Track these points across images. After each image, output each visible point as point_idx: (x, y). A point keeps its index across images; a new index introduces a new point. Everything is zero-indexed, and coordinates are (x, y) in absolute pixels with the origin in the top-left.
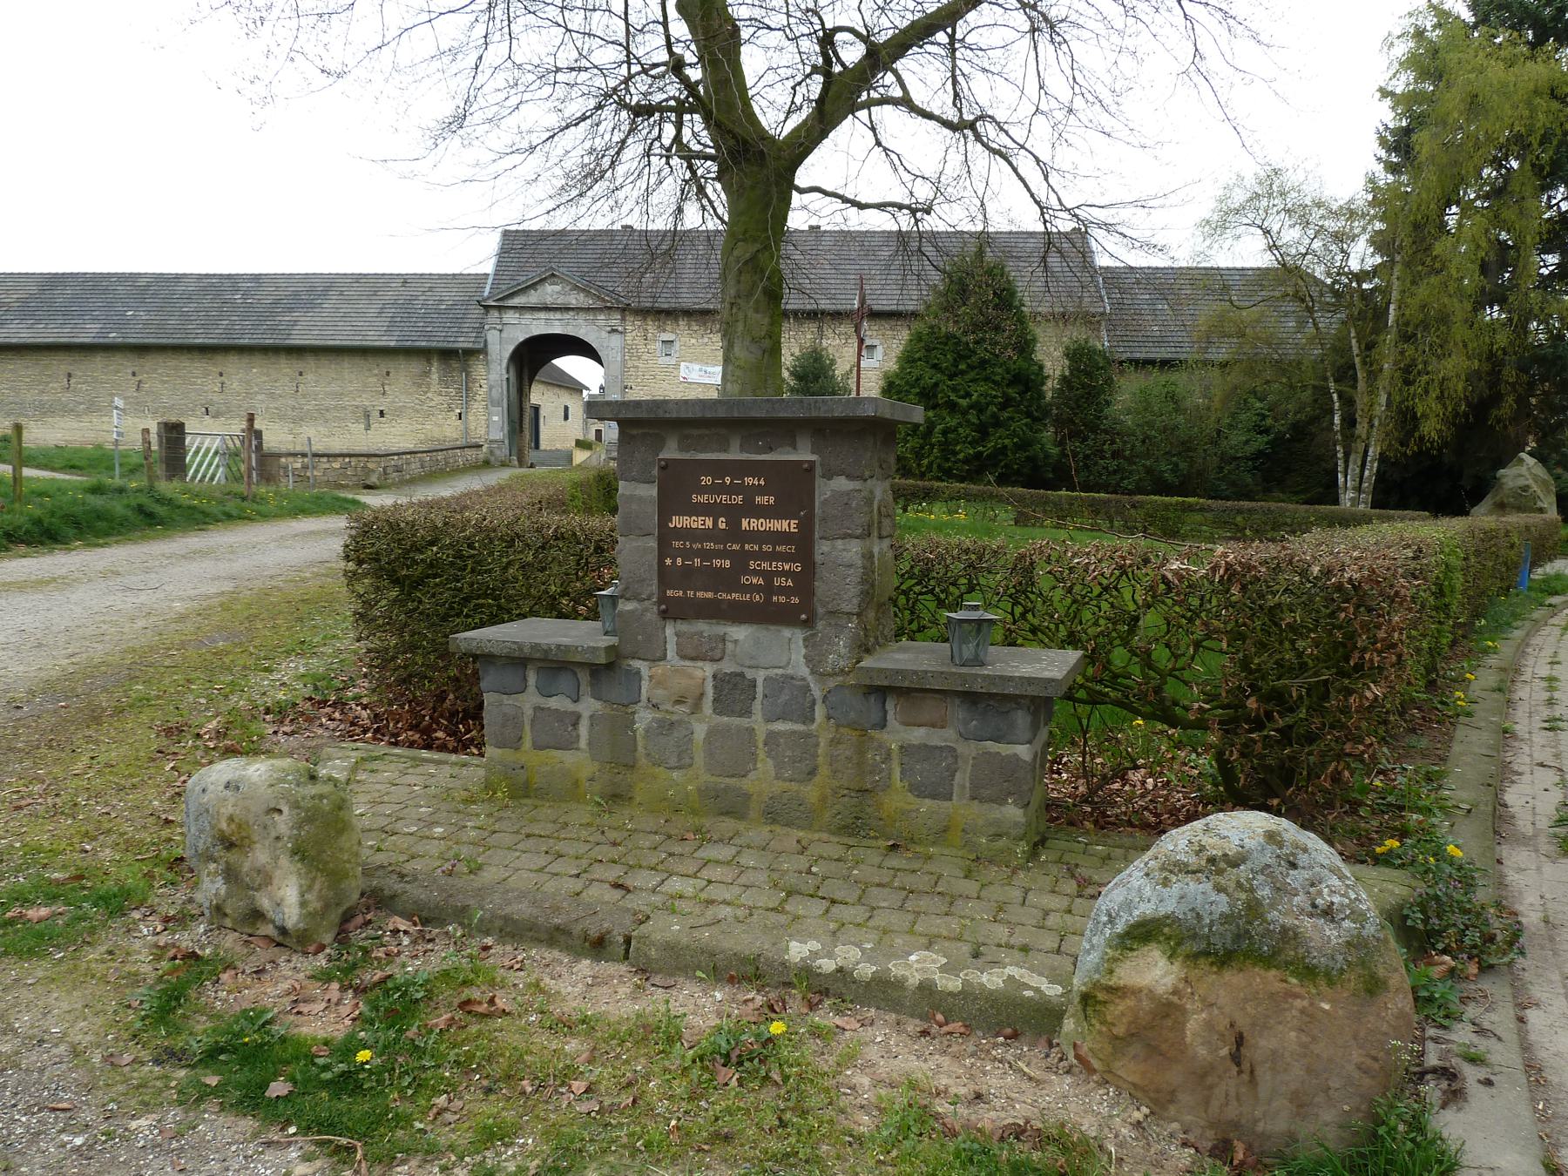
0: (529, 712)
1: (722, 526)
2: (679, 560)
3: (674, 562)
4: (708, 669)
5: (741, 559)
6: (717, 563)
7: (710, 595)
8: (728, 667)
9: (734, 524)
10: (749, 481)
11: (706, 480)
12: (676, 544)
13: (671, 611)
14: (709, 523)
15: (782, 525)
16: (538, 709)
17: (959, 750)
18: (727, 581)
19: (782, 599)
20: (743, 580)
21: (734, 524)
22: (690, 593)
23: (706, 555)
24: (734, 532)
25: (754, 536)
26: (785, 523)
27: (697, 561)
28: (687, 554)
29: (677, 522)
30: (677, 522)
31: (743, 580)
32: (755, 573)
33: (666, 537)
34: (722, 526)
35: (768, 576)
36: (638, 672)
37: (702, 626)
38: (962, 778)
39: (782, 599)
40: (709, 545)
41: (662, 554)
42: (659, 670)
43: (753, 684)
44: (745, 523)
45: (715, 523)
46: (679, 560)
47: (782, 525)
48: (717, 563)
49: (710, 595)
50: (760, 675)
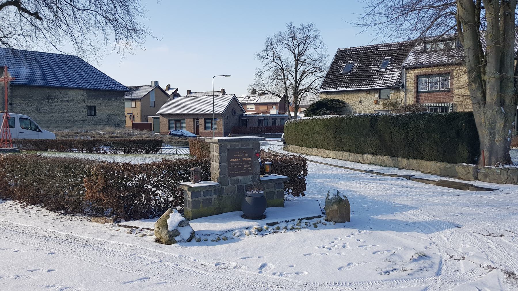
0: (202, 200)
4: (236, 185)
5: (242, 165)
8: (239, 184)
9: (241, 159)
11: (236, 152)
13: (230, 176)
21: (241, 159)
23: (236, 165)
28: (233, 166)
29: (232, 160)
30: (232, 160)
33: (229, 162)
35: (247, 168)
37: (235, 178)
38: (275, 196)
41: (229, 166)
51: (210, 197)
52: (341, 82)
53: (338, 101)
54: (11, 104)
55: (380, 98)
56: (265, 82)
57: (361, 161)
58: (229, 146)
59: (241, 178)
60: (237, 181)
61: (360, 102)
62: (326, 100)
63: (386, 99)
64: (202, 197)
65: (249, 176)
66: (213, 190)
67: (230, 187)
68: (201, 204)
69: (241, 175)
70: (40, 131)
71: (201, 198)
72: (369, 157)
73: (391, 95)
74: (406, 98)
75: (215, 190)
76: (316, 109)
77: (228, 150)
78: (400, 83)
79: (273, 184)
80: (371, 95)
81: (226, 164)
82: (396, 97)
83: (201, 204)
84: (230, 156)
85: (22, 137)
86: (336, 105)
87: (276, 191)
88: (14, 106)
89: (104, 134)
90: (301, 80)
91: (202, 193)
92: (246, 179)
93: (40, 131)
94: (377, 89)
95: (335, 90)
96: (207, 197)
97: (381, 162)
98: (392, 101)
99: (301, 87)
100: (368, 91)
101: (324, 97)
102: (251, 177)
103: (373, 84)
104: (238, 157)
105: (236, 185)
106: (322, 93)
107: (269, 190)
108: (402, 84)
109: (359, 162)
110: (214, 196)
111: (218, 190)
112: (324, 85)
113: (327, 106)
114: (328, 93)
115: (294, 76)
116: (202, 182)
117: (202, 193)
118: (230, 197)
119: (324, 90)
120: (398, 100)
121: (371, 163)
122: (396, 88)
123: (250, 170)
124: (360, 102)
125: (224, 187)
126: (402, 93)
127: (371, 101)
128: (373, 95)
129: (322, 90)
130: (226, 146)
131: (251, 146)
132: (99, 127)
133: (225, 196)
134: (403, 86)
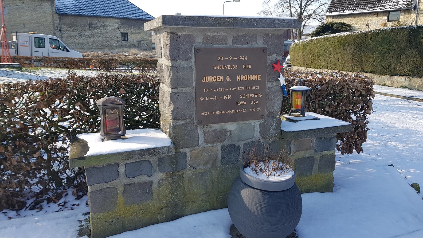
0: (121, 189)
1: (228, 80)
2: (207, 98)
3: (205, 98)
6: (226, 97)
7: (222, 112)
8: (227, 142)
9: (233, 78)
10: (240, 58)
11: (220, 58)
12: (206, 90)
14: (222, 79)
15: (254, 77)
16: (126, 186)
17: (315, 157)
18: (230, 104)
19: (254, 110)
20: (237, 103)
21: (233, 78)
22: (213, 113)
23: (220, 94)
24: (234, 83)
25: (242, 83)
26: (256, 77)
27: (216, 97)
28: (211, 95)
29: (207, 79)
30: (207, 79)
31: (237, 103)
32: (243, 100)
33: (200, 85)
34: (228, 80)
35: (248, 100)
36: (185, 153)
37: (216, 126)
38: (316, 167)
39: (254, 110)
40: (222, 89)
42: (196, 150)
43: (239, 147)
44: (238, 78)
45: (225, 78)
46: (207, 98)
47: (254, 77)
48: (226, 97)
49: (222, 112)
50: (242, 144)
51: (146, 179)
52: (348, 5)
53: (344, 24)
54: (60, 30)
55: (388, 20)
56: (272, 9)
57: (388, 83)
58: (199, 41)
59: (231, 126)
60: (221, 136)
61: (367, 25)
62: (332, 24)
63: (395, 21)
64: (123, 180)
65: (252, 122)
66: (154, 160)
67: (204, 148)
68: (120, 199)
69: (233, 119)
70: (68, 51)
71: (119, 184)
72: (401, 79)
73: (401, 17)
74: (417, 20)
75: (160, 160)
76: (321, 33)
77: (198, 51)
78: (412, 5)
79: (312, 141)
80: (379, 18)
81: (191, 90)
82: (406, 19)
83: (120, 199)
84: (203, 69)
85: (52, 55)
86: (343, 28)
87: (317, 156)
88: (63, 32)
89: (129, 55)
90: (305, 8)
91: (122, 169)
92: (245, 130)
93: (68, 51)
94: (386, 12)
95: (342, 13)
96: (137, 180)
97: (419, 86)
98: (402, 23)
99: (305, 14)
100: (377, 14)
101: (330, 20)
102: (257, 123)
103: (383, 6)
104: (224, 73)
105: (219, 146)
106: (327, 17)
107: (301, 154)
108: (414, 5)
109: (385, 85)
110: (158, 176)
111: (167, 160)
112: (330, 9)
113: (333, 29)
114: (334, 17)
115: (300, 3)
116: (129, 134)
117: (122, 169)
118: (202, 174)
119: (331, 14)
120: (408, 22)
121: (402, 87)
122: (407, 10)
123: (256, 106)
124: (367, 25)
125: (187, 151)
126: (414, 15)
127: (379, 23)
128: (381, 17)
129: (328, 14)
130: (191, 40)
131: (260, 43)
132: (126, 50)
133: (188, 173)
134: (415, 8)
